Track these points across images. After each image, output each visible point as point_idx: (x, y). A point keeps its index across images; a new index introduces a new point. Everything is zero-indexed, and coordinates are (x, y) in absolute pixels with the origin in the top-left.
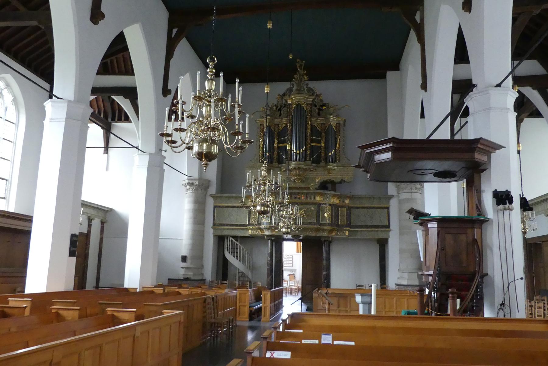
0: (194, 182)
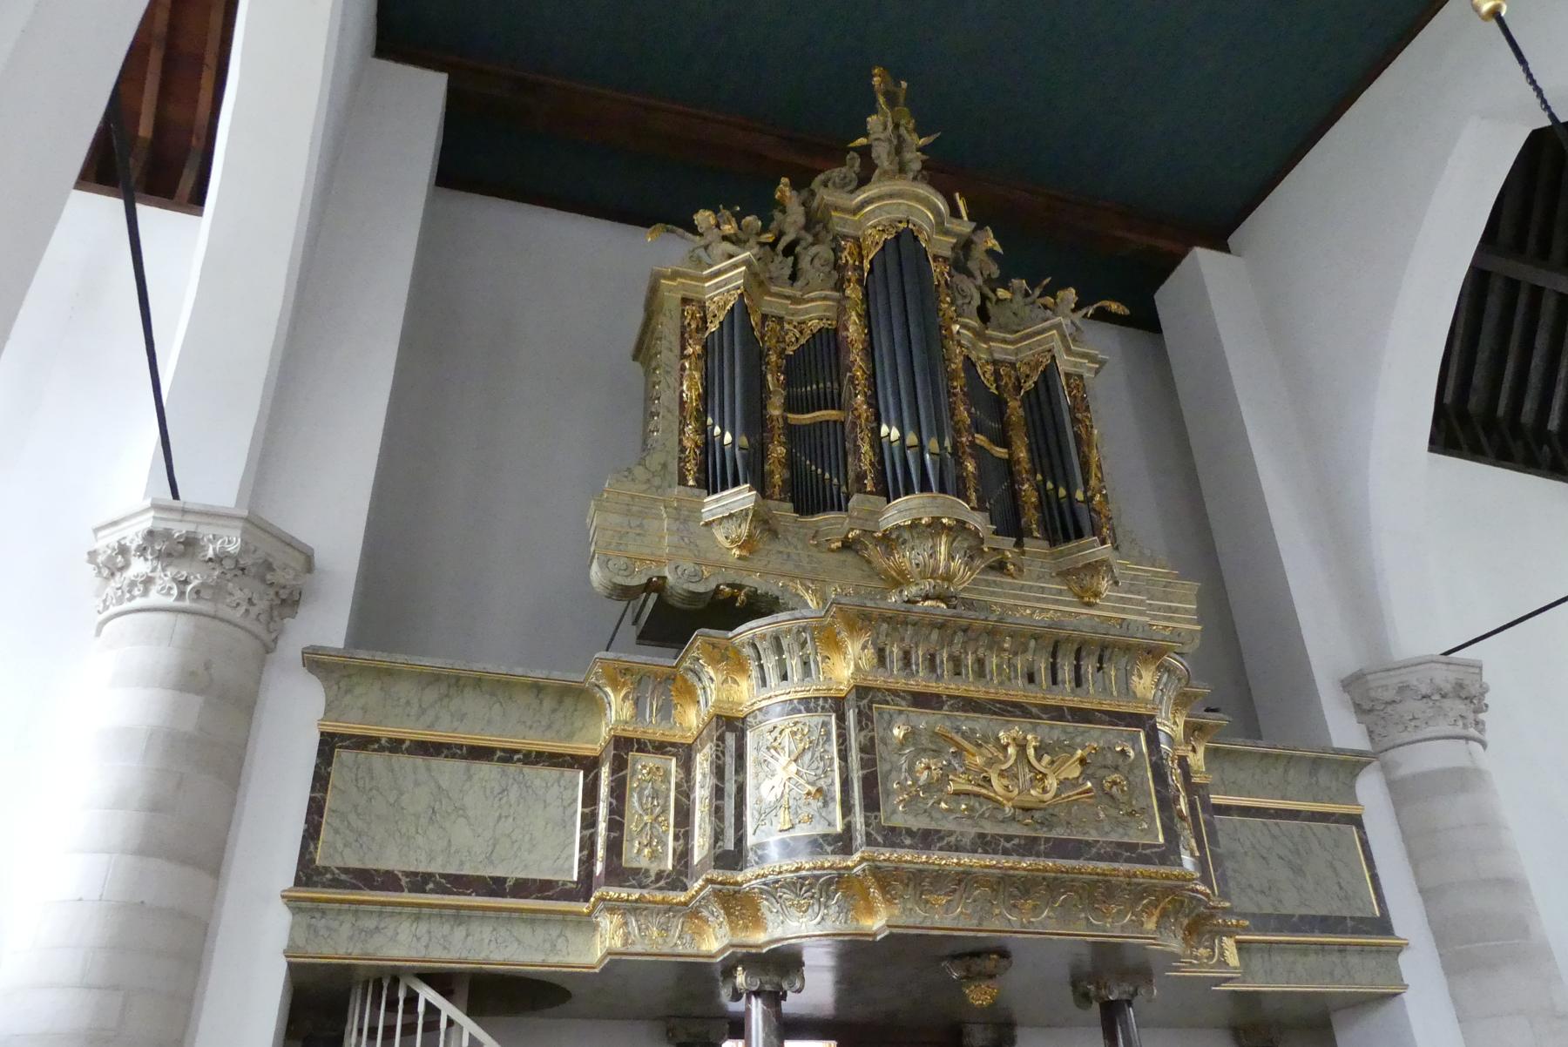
0: (205, 531)
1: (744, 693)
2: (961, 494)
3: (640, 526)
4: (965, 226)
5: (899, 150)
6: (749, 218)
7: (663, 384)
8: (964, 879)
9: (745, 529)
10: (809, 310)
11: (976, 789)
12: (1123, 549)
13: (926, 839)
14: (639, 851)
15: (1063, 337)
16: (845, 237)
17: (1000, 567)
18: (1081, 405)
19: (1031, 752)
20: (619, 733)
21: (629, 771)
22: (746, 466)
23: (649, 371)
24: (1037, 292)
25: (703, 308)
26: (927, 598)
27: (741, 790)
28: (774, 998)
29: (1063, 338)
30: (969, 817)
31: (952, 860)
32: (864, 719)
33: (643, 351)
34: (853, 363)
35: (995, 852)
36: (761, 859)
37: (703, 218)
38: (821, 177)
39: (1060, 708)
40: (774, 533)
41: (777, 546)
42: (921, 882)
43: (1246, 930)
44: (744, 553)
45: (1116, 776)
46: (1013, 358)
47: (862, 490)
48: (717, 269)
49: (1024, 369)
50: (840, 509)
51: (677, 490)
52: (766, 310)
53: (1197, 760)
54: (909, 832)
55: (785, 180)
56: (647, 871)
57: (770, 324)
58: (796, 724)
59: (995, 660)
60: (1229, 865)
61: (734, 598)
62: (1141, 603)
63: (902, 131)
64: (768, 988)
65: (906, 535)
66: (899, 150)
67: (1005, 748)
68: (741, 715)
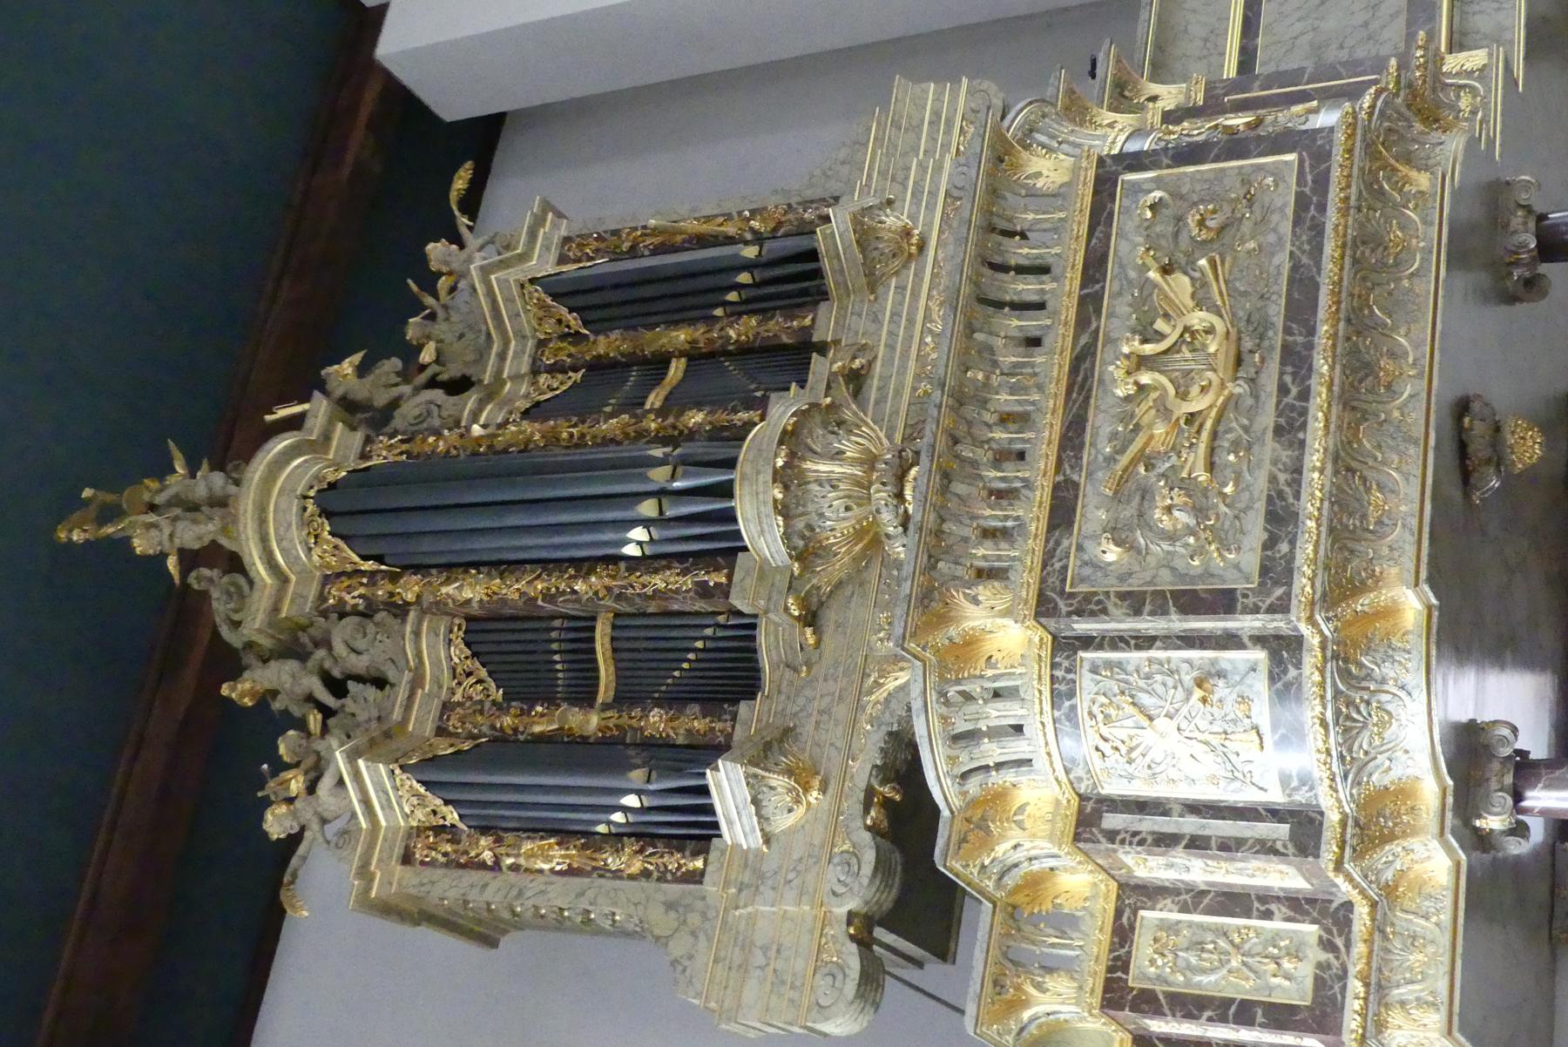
1: (1040, 796)
2: (738, 434)
3: (765, 949)
4: (318, 409)
5: (193, 507)
6: (282, 750)
7: (538, 901)
8: (1345, 462)
9: (778, 781)
10: (433, 658)
11: (1205, 435)
12: (834, 187)
13: (1281, 518)
14: (1288, 977)
15: (504, 264)
16: (322, 598)
17: (856, 380)
18: (609, 243)
19: (1149, 349)
20: (1096, 1000)
21: (1158, 988)
22: (678, 772)
23: (517, 923)
24: (429, 300)
25: (420, 831)
26: (900, 496)
27: (1195, 808)
28: (1525, 769)
29: (502, 265)
30: (1249, 448)
31: (1315, 481)
32: (1089, 606)
33: (483, 932)
34: (522, 594)
35: (1304, 412)
36: (1306, 781)
37: (276, 824)
38: (225, 632)
39: (1082, 301)
40: (787, 733)
41: (808, 729)
42: (1348, 532)
43: (1432, 36)
44: (816, 783)
45: (1192, 220)
46: (530, 343)
47: (724, 591)
48: (358, 806)
49: (549, 327)
50: (753, 626)
51: (710, 887)
52: (429, 728)
53: (1169, 95)
54: (1270, 543)
55: (225, 690)
56: (1319, 966)
57: (453, 723)
58: (1092, 715)
59: (1003, 397)
60: (1333, 55)
61: (887, 803)
62: (922, 168)
63: (160, 499)
64: (1509, 779)
65: (800, 524)
66: (193, 507)
67: (1141, 388)
68: (1075, 802)
